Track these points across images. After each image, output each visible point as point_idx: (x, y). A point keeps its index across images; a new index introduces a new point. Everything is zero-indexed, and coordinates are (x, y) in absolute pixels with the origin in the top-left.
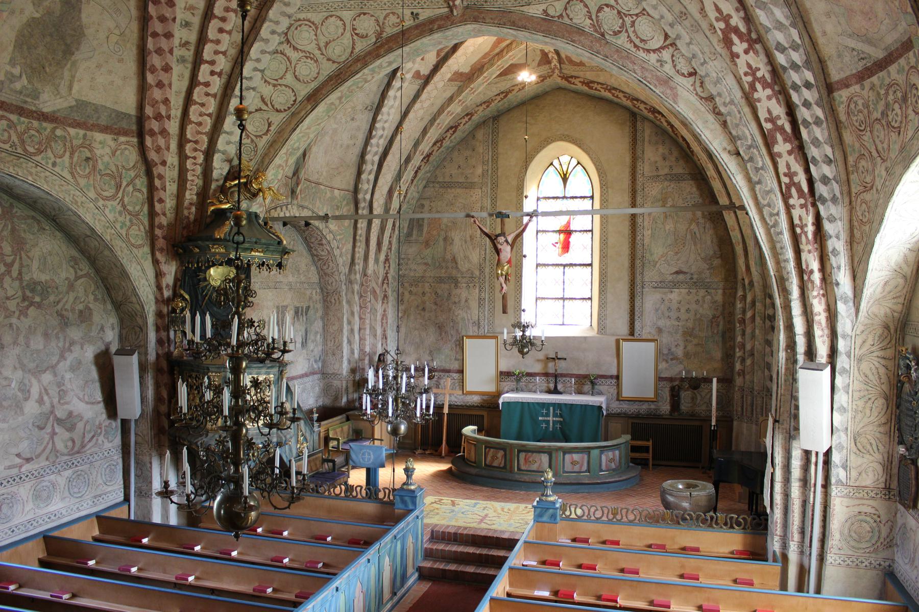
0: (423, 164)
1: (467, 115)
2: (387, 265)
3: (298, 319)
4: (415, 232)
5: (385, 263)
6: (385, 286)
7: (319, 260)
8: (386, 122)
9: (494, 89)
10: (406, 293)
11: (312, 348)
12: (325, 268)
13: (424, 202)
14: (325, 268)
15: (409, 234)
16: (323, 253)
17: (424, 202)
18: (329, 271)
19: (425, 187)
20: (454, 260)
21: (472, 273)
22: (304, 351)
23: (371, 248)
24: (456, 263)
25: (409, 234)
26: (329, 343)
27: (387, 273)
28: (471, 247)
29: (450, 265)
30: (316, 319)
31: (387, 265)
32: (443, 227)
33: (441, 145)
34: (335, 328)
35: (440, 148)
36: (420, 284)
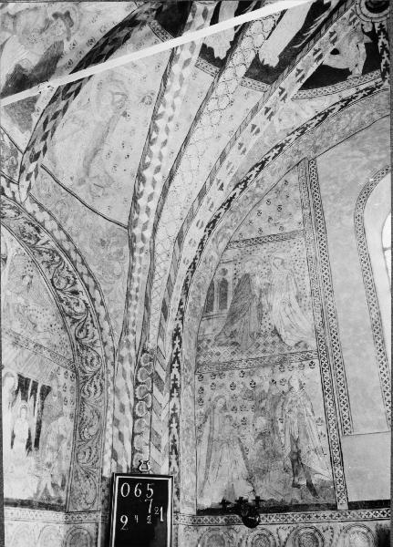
0: (222, 210)
1: (276, 147)
2: (177, 341)
3: (25, 398)
4: (216, 305)
5: (174, 339)
6: (175, 371)
7: (73, 323)
8: (170, 119)
9: (308, 109)
10: (207, 388)
11: (48, 460)
12: (81, 335)
13: (227, 267)
14: (81, 335)
15: (209, 307)
16: (78, 310)
17: (227, 267)
18: (87, 341)
19: (227, 248)
20: (275, 332)
21: (306, 346)
22: (32, 460)
23: (153, 311)
24: (279, 336)
25: (209, 307)
26: (81, 456)
27: (177, 353)
28: (298, 310)
29: (270, 339)
30: (61, 414)
31: (177, 341)
32: (256, 292)
33: (245, 186)
34: (92, 431)
35: (243, 189)
36: (227, 373)
